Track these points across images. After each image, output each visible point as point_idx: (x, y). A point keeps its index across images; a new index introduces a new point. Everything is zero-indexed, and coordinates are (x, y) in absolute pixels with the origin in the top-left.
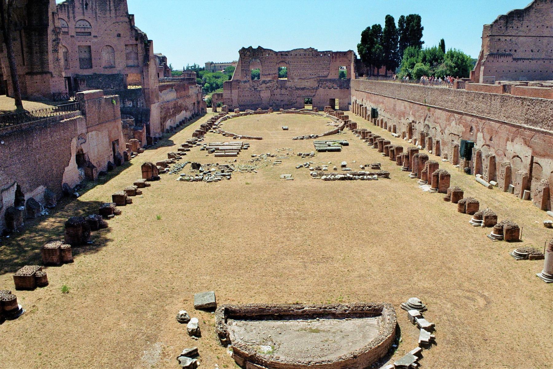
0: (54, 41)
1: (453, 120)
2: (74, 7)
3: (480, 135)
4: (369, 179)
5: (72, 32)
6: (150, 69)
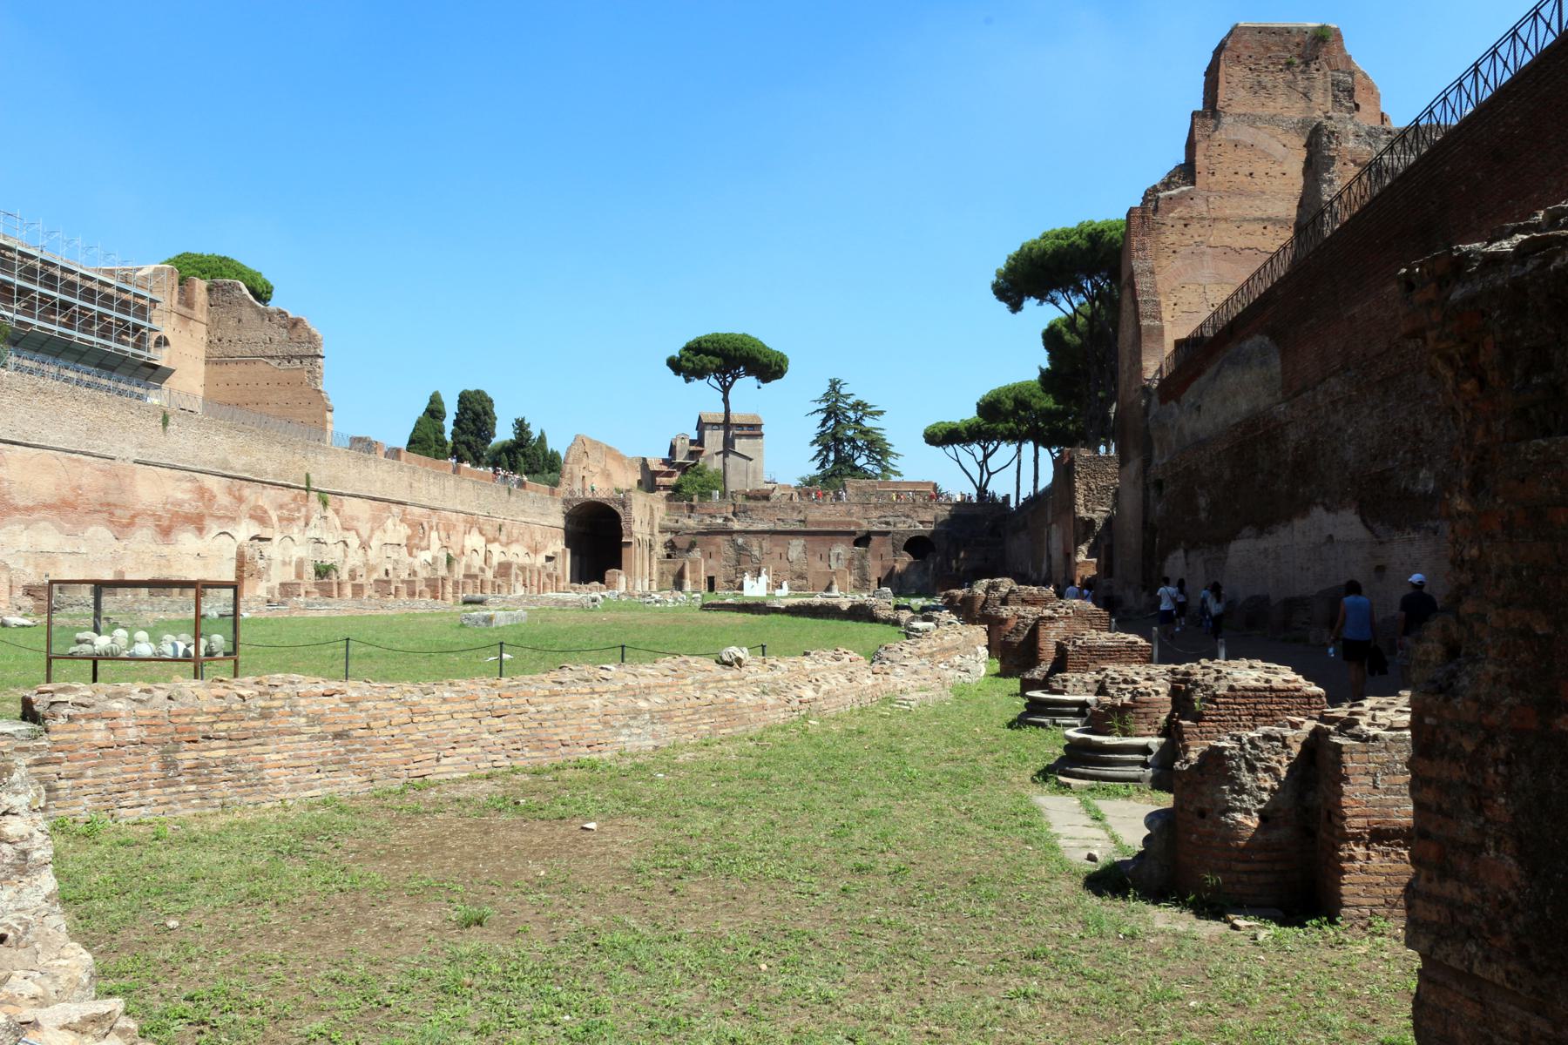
1: (389, 517)
3: (434, 535)
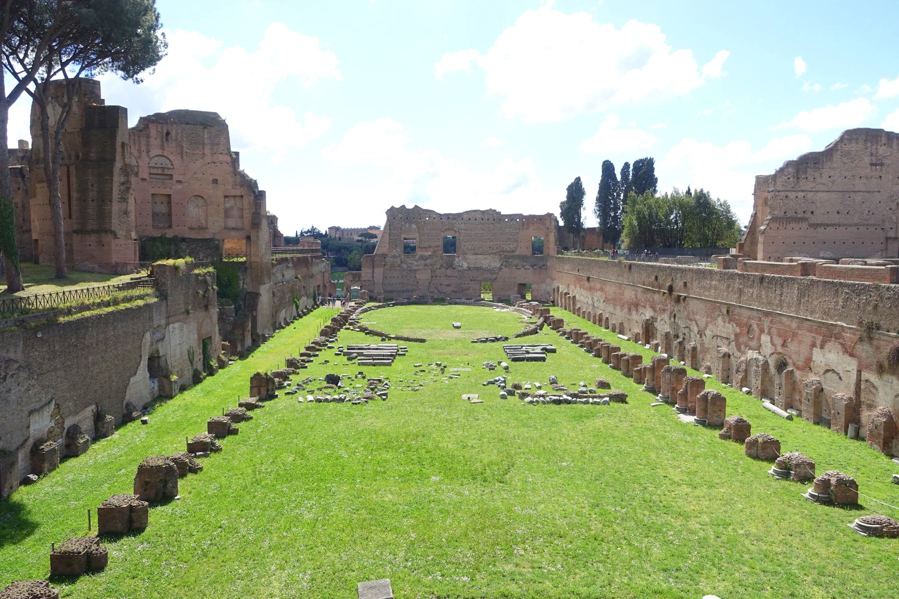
0: (123, 184)
1: (719, 315)
2: (148, 136)
3: (765, 338)
4: (595, 403)
5: (144, 174)
6: (260, 233)
